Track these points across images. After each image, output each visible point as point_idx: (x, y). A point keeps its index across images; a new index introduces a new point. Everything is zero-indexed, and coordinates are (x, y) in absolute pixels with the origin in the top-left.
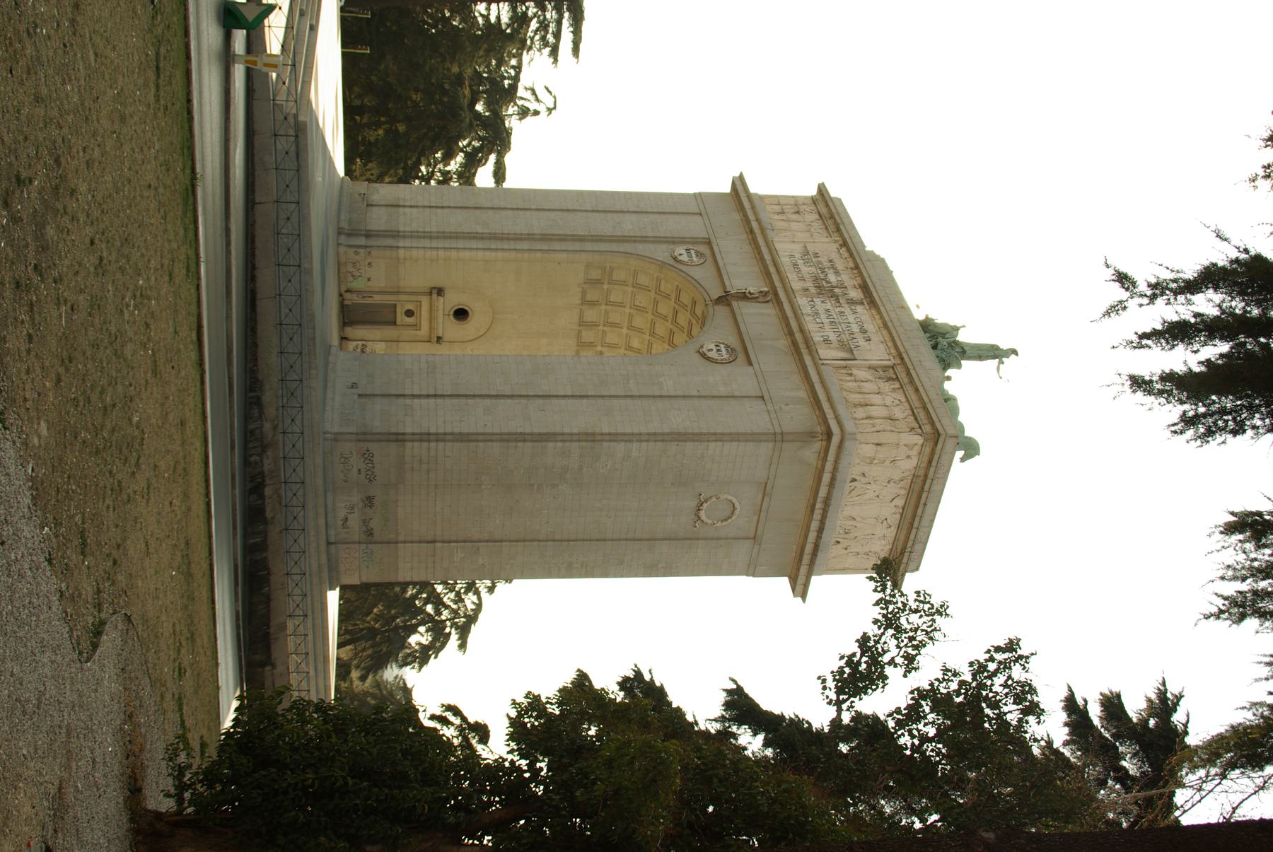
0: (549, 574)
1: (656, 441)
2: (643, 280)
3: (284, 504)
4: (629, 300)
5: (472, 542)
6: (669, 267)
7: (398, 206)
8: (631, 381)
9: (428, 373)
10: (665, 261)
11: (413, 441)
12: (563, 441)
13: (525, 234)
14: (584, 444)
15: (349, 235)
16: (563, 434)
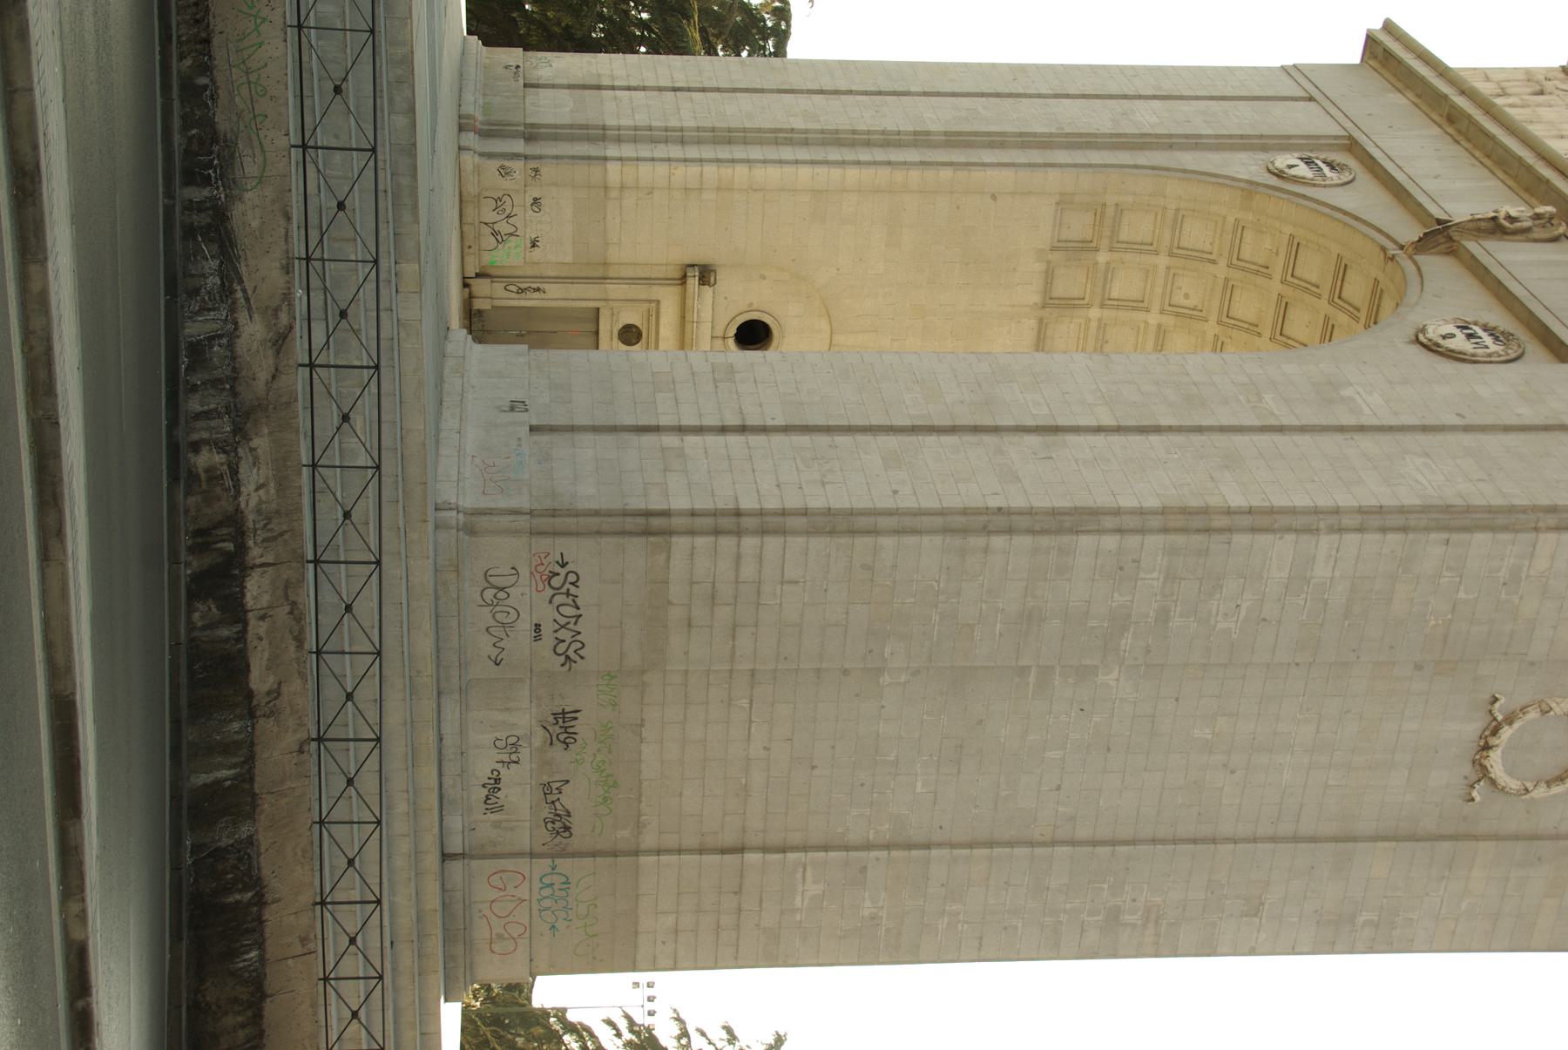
0: (1052, 947)
1: (1384, 530)
2: (1196, 235)
3: (311, 643)
4: (1159, 290)
5: (847, 848)
6: (1270, 192)
7: (599, 87)
8: (1268, 397)
9: (715, 380)
10: (1255, 179)
11: (691, 533)
12: (1119, 531)
13: (907, 133)
14: (1180, 539)
15: (486, 134)
16: (1117, 512)
